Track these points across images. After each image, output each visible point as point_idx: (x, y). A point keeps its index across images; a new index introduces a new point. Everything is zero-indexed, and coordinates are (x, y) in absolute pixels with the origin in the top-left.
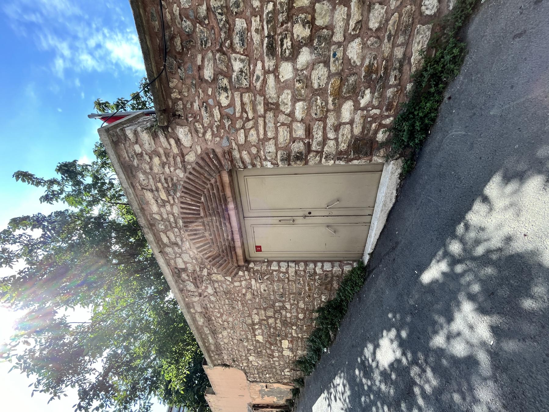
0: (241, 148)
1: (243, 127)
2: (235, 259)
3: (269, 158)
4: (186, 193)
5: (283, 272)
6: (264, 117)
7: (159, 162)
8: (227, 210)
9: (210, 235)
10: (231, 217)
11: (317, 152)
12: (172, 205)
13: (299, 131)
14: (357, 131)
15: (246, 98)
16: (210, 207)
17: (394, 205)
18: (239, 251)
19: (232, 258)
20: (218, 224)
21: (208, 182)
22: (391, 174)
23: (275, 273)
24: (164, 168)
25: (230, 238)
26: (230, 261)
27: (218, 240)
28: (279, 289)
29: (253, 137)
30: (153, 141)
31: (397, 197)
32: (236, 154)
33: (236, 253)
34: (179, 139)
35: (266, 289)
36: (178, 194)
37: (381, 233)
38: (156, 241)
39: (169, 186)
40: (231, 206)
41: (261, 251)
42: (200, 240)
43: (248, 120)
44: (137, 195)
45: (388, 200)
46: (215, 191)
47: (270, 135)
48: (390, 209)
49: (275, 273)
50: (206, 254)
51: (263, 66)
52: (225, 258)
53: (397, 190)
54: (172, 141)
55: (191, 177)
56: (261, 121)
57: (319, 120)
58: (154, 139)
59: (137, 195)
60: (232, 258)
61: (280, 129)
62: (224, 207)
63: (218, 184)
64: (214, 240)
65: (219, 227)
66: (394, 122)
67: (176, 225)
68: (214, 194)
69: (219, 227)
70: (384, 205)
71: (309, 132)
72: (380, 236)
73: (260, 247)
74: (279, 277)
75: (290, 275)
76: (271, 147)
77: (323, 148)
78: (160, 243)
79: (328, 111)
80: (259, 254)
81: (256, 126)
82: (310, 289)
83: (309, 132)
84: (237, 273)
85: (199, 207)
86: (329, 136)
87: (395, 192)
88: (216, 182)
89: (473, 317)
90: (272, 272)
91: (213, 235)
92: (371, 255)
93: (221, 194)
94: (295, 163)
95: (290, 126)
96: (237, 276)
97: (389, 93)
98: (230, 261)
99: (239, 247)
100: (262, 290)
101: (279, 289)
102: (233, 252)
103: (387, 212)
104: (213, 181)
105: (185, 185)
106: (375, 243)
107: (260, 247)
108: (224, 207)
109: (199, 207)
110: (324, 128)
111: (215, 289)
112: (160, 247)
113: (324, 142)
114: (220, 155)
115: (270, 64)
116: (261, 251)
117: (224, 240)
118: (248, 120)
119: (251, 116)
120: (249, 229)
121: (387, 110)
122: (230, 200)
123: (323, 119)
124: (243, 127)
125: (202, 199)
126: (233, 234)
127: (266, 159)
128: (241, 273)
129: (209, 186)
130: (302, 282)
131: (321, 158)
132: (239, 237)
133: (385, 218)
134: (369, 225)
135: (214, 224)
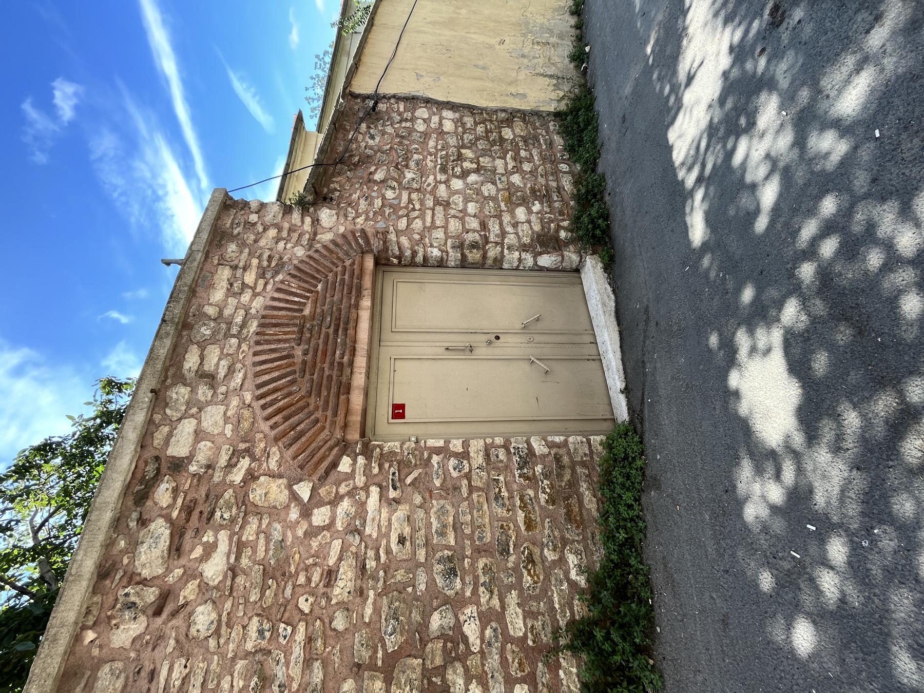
0: (398, 233)
1: (407, 215)
2: (340, 418)
3: (435, 244)
4: (294, 276)
5: (456, 455)
6: (433, 210)
7: (275, 235)
8: (357, 306)
9: (305, 353)
10: (359, 320)
11: (497, 244)
12: (255, 295)
13: (474, 224)
14: (537, 228)
15: (414, 196)
16: (328, 300)
17: (616, 302)
18: (357, 399)
19: (335, 414)
20: (331, 331)
21: (340, 264)
22: (593, 274)
23: (435, 459)
24: (277, 243)
25: (346, 359)
26: (327, 425)
27: (319, 365)
28: (442, 533)
29: (418, 224)
30: (281, 215)
31: (614, 291)
32: (392, 237)
33: (348, 400)
34: (318, 220)
35: (407, 531)
36: (280, 277)
37: (621, 347)
38: (167, 364)
39: (269, 266)
40: (366, 302)
41: (402, 416)
42: (276, 364)
43: (414, 209)
44: (202, 269)
45: (605, 298)
46: (346, 277)
47: (438, 223)
48: (613, 309)
49: (435, 459)
50: (271, 403)
51: (435, 179)
52: (319, 414)
53: (609, 284)
54: (308, 220)
55: (316, 256)
56: (429, 212)
57: (495, 216)
58: (283, 215)
59: (202, 269)
60: (335, 414)
61: (452, 221)
62: (353, 301)
63: (355, 267)
64: (309, 364)
65: (331, 337)
66: (571, 224)
67: (240, 332)
68: (343, 280)
69: (331, 337)
70: (604, 304)
71: (484, 226)
72: (622, 351)
73: (402, 406)
74: (446, 475)
75: (475, 465)
76: (439, 234)
77: (503, 240)
78: (172, 371)
79: (501, 211)
80: (399, 428)
81: (422, 217)
82: (529, 524)
83: (484, 226)
84: (335, 465)
85: (308, 298)
86: (507, 229)
87: (608, 287)
88: (353, 264)
89: (757, 150)
90: (430, 458)
91: (310, 356)
92: (626, 391)
93: (355, 281)
94: (471, 252)
95: (462, 219)
96: (333, 477)
97: (557, 205)
98: (327, 425)
99: (358, 388)
100: (394, 538)
101: (442, 533)
102: (342, 397)
103: (613, 314)
104: (348, 263)
105: (300, 265)
106: (621, 367)
107: (402, 406)
108: (353, 301)
109: (308, 298)
110: (501, 224)
111: (389, 98)
112: (165, 381)
113: (503, 234)
114: (369, 235)
115: (442, 177)
116: (402, 416)
117: (332, 364)
118: (414, 209)
119: (417, 207)
120: (385, 365)
121: (560, 215)
122: (367, 293)
123: (499, 216)
124: (407, 215)
125: (319, 287)
126: (354, 355)
127: (432, 246)
128: (345, 465)
129: (340, 269)
130: (505, 494)
131: (503, 248)
132: (364, 365)
133: (615, 323)
134: (598, 359)
135: (324, 330)
